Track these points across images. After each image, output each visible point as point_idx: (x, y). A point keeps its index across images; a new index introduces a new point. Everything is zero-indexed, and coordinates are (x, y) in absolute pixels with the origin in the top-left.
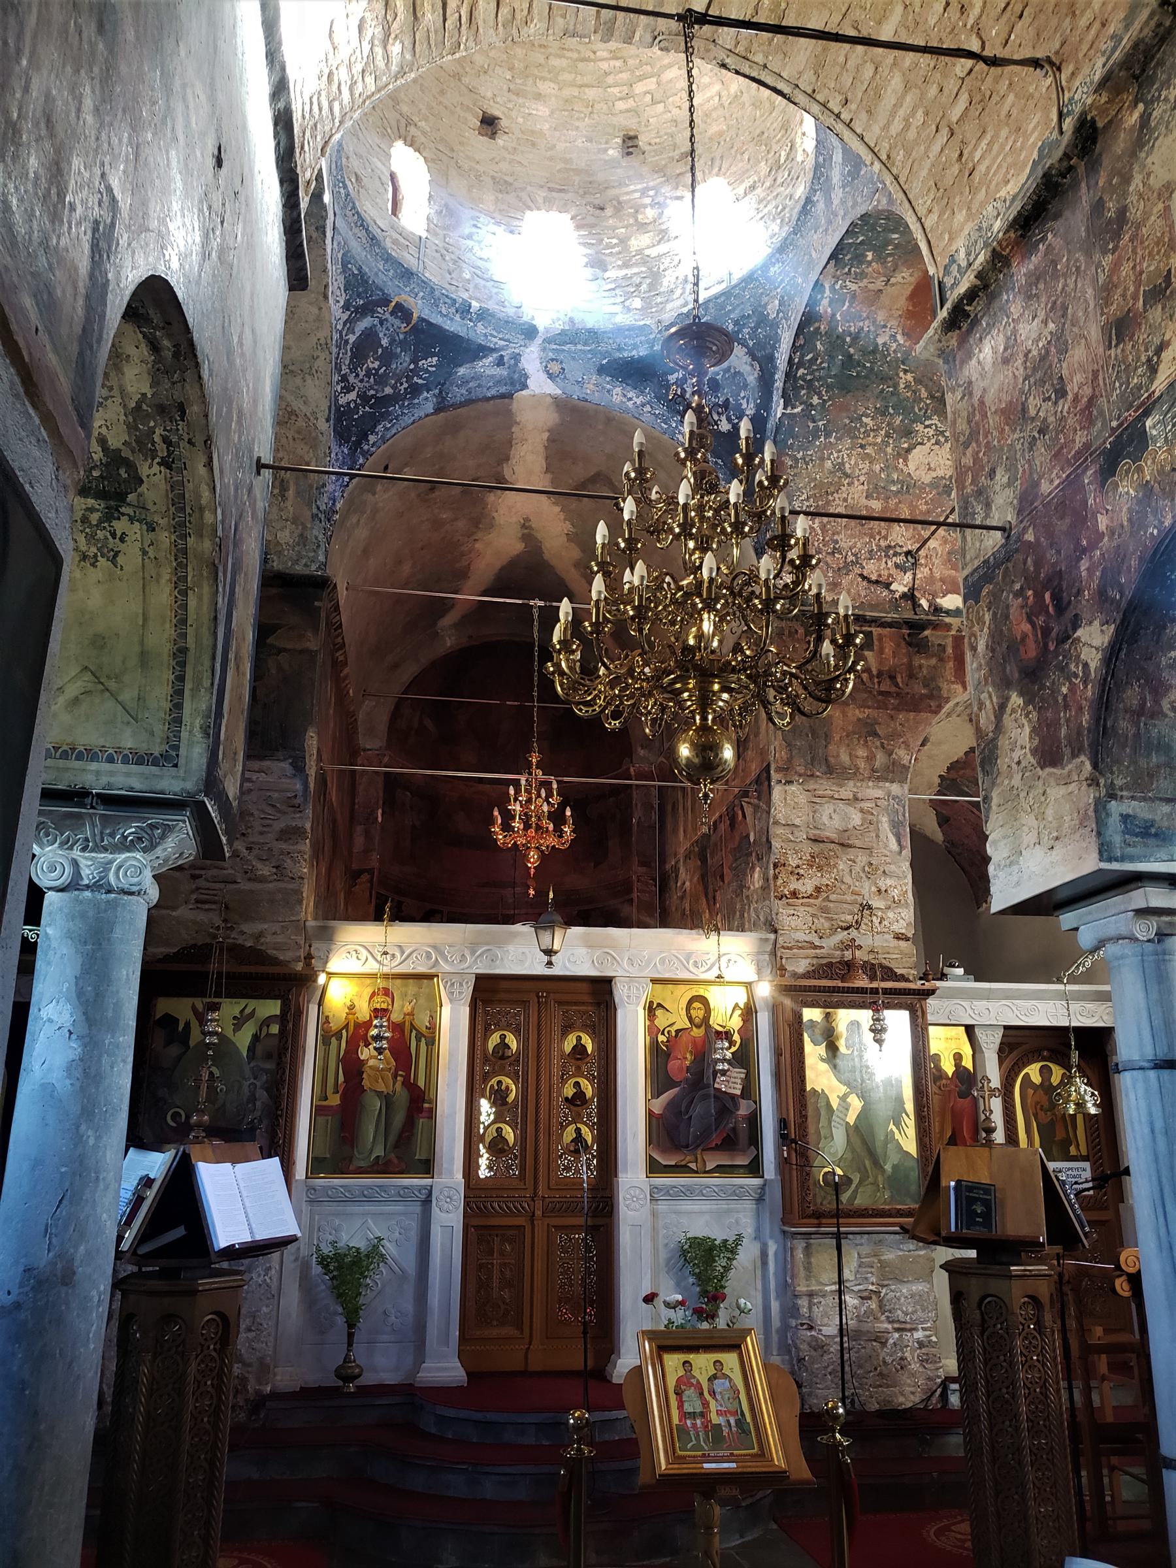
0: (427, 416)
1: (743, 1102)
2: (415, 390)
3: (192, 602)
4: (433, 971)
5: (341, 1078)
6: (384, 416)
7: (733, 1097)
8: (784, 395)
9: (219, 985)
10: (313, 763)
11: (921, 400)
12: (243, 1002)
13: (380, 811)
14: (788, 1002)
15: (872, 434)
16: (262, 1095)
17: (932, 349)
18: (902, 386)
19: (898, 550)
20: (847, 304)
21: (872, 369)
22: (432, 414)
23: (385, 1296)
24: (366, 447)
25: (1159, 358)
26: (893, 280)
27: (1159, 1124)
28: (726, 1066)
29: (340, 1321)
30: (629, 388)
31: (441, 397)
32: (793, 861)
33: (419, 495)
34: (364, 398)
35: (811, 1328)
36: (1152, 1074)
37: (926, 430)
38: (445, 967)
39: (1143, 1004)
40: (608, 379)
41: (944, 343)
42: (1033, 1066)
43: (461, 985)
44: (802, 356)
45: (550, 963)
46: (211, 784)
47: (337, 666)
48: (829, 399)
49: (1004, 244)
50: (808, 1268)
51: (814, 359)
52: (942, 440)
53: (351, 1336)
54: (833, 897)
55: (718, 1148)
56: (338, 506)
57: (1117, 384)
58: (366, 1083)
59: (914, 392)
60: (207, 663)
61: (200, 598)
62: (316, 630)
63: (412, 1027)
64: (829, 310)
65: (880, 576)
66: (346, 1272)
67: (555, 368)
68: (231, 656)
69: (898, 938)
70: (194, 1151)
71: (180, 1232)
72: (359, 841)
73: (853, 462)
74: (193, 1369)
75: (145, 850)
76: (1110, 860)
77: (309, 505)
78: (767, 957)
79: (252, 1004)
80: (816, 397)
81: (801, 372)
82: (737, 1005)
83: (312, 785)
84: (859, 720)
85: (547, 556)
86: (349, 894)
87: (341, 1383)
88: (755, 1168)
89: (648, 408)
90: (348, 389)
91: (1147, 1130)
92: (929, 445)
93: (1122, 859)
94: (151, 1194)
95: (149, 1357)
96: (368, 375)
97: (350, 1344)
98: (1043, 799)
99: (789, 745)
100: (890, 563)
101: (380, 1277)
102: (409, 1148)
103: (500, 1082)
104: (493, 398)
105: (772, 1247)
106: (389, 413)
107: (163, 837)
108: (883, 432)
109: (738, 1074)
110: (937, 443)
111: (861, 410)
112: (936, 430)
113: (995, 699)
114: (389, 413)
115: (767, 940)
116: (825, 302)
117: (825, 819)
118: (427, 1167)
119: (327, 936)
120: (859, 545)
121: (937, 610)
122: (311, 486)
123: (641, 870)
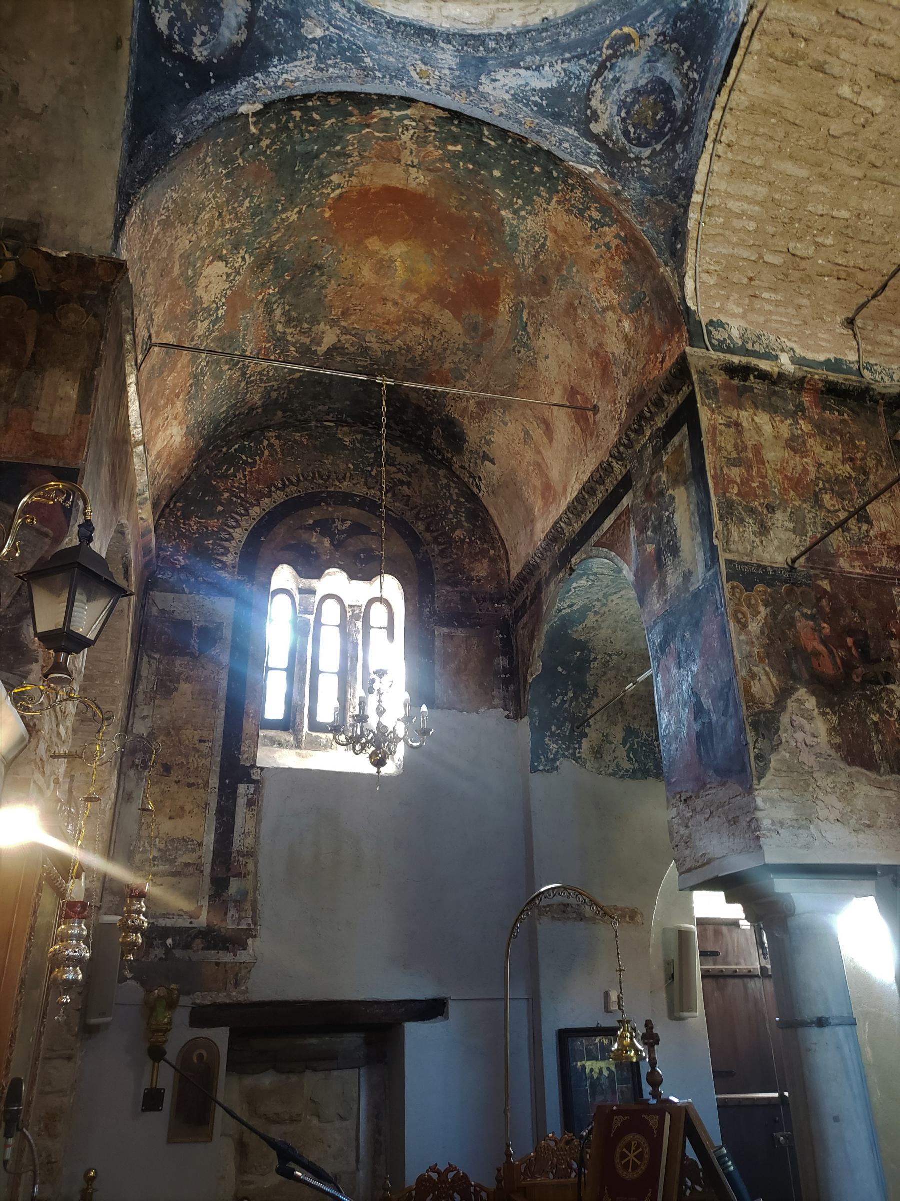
17: (701, 363)
18: (284, 216)
20: (381, 135)
26: (413, 171)
37: (240, 260)
41: (712, 371)
44: (315, 108)
49: (812, 382)
51: (313, 122)
52: (232, 278)
59: (278, 229)
64: (376, 120)
80: (268, 141)
81: (297, 114)
108: (236, 224)
110: (228, 275)
116: (386, 113)
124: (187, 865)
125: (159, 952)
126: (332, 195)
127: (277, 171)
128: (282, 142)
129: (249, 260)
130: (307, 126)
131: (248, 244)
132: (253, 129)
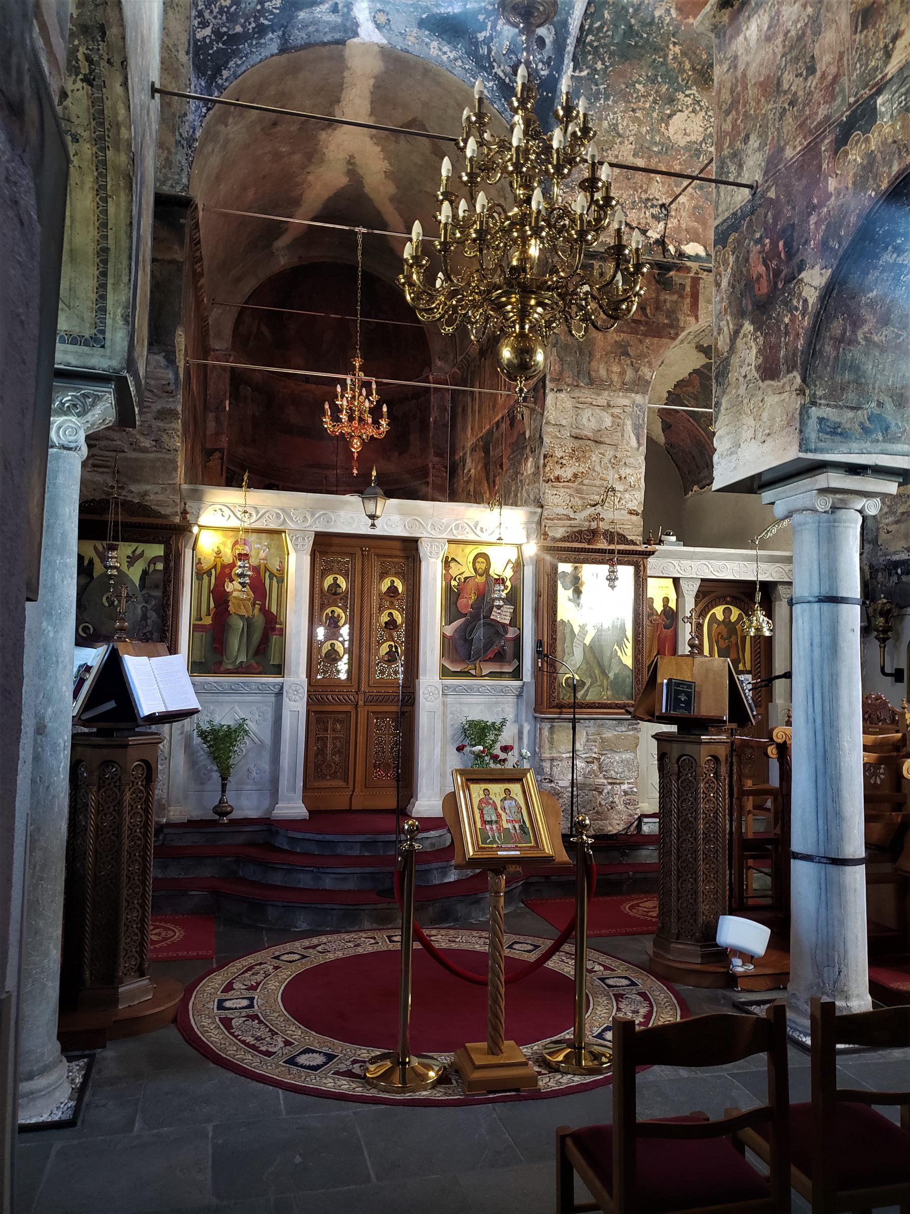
0: (272, 56)
1: (511, 629)
2: (261, 30)
3: (111, 209)
4: (281, 528)
5: (212, 605)
6: (236, 53)
7: (503, 625)
8: (574, 59)
9: (116, 531)
10: (182, 357)
11: (685, 71)
12: (134, 545)
13: (227, 402)
14: (548, 558)
15: (642, 100)
16: (152, 616)
18: (671, 57)
19: (655, 202)
21: (648, 39)
22: (277, 54)
23: (248, 760)
24: (220, 82)
25: (894, 44)
27: (817, 640)
28: (501, 603)
29: (216, 776)
30: (444, 43)
31: (284, 39)
32: (558, 454)
33: (263, 129)
34: (216, 32)
35: (551, 781)
36: (816, 606)
38: (292, 525)
39: (815, 556)
40: (427, 33)
41: (717, 19)
42: (718, 608)
43: (304, 539)
45: (373, 525)
46: (130, 363)
47: (197, 276)
48: (611, 66)
50: (551, 742)
51: (602, 27)
52: (698, 108)
53: (224, 786)
54: (586, 482)
55: (490, 660)
56: (198, 134)
57: (858, 65)
58: (231, 609)
60: (125, 262)
61: (118, 206)
62: (182, 244)
63: (266, 569)
65: (639, 223)
66: (220, 743)
67: (382, 18)
68: (141, 258)
69: (631, 513)
70: (120, 647)
71: (111, 705)
72: (211, 425)
73: (625, 124)
74: (128, 796)
75: (79, 415)
76: (806, 451)
77: (173, 132)
78: (534, 526)
79: (141, 547)
80: (600, 63)
81: (590, 38)
82: (509, 561)
83: (181, 375)
84: (616, 342)
85: (367, 190)
86: (205, 467)
87: (217, 817)
88: (517, 674)
89: (459, 63)
90: (204, 24)
91: (808, 644)
92: (686, 112)
93: (815, 451)
94: (90, 678)
95: (95, 788)
96: (221, 12)
97: (224, 791)
98: (761, 404)
99: (561, 360)
100: (647, 213)
101: (244, 746)
102: (265, 653)
103: (333, 612)
104: (329, 43)
105: (527, 728)
106: (240, 51)
107: (93, 405)
108: (651, 99)
109: (508, 609)
110: (693, 111)
111: (635, 77)
112: (694, 99)
113: (731, 326)
114: (240, 51)
115: (535, 513)
117: (585, 421)
118: (279, 670)
119: (198, 497)
120: (625, 196)
121: (681, 255)
122: (174, 114)
123: (436, 459)
124: (903, 513)
125: (895, 579)
126: (674, 16)
127: (626, 60)
128: (606, 52)
129: (694, 90)
130: (601, 32)
131: (676, 90)
132: (584, 73)
